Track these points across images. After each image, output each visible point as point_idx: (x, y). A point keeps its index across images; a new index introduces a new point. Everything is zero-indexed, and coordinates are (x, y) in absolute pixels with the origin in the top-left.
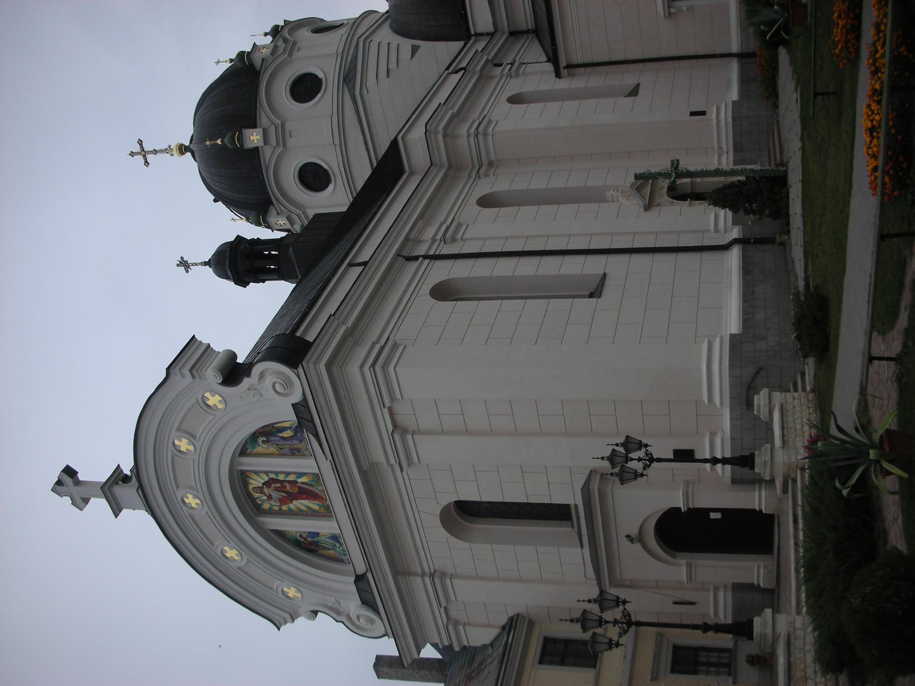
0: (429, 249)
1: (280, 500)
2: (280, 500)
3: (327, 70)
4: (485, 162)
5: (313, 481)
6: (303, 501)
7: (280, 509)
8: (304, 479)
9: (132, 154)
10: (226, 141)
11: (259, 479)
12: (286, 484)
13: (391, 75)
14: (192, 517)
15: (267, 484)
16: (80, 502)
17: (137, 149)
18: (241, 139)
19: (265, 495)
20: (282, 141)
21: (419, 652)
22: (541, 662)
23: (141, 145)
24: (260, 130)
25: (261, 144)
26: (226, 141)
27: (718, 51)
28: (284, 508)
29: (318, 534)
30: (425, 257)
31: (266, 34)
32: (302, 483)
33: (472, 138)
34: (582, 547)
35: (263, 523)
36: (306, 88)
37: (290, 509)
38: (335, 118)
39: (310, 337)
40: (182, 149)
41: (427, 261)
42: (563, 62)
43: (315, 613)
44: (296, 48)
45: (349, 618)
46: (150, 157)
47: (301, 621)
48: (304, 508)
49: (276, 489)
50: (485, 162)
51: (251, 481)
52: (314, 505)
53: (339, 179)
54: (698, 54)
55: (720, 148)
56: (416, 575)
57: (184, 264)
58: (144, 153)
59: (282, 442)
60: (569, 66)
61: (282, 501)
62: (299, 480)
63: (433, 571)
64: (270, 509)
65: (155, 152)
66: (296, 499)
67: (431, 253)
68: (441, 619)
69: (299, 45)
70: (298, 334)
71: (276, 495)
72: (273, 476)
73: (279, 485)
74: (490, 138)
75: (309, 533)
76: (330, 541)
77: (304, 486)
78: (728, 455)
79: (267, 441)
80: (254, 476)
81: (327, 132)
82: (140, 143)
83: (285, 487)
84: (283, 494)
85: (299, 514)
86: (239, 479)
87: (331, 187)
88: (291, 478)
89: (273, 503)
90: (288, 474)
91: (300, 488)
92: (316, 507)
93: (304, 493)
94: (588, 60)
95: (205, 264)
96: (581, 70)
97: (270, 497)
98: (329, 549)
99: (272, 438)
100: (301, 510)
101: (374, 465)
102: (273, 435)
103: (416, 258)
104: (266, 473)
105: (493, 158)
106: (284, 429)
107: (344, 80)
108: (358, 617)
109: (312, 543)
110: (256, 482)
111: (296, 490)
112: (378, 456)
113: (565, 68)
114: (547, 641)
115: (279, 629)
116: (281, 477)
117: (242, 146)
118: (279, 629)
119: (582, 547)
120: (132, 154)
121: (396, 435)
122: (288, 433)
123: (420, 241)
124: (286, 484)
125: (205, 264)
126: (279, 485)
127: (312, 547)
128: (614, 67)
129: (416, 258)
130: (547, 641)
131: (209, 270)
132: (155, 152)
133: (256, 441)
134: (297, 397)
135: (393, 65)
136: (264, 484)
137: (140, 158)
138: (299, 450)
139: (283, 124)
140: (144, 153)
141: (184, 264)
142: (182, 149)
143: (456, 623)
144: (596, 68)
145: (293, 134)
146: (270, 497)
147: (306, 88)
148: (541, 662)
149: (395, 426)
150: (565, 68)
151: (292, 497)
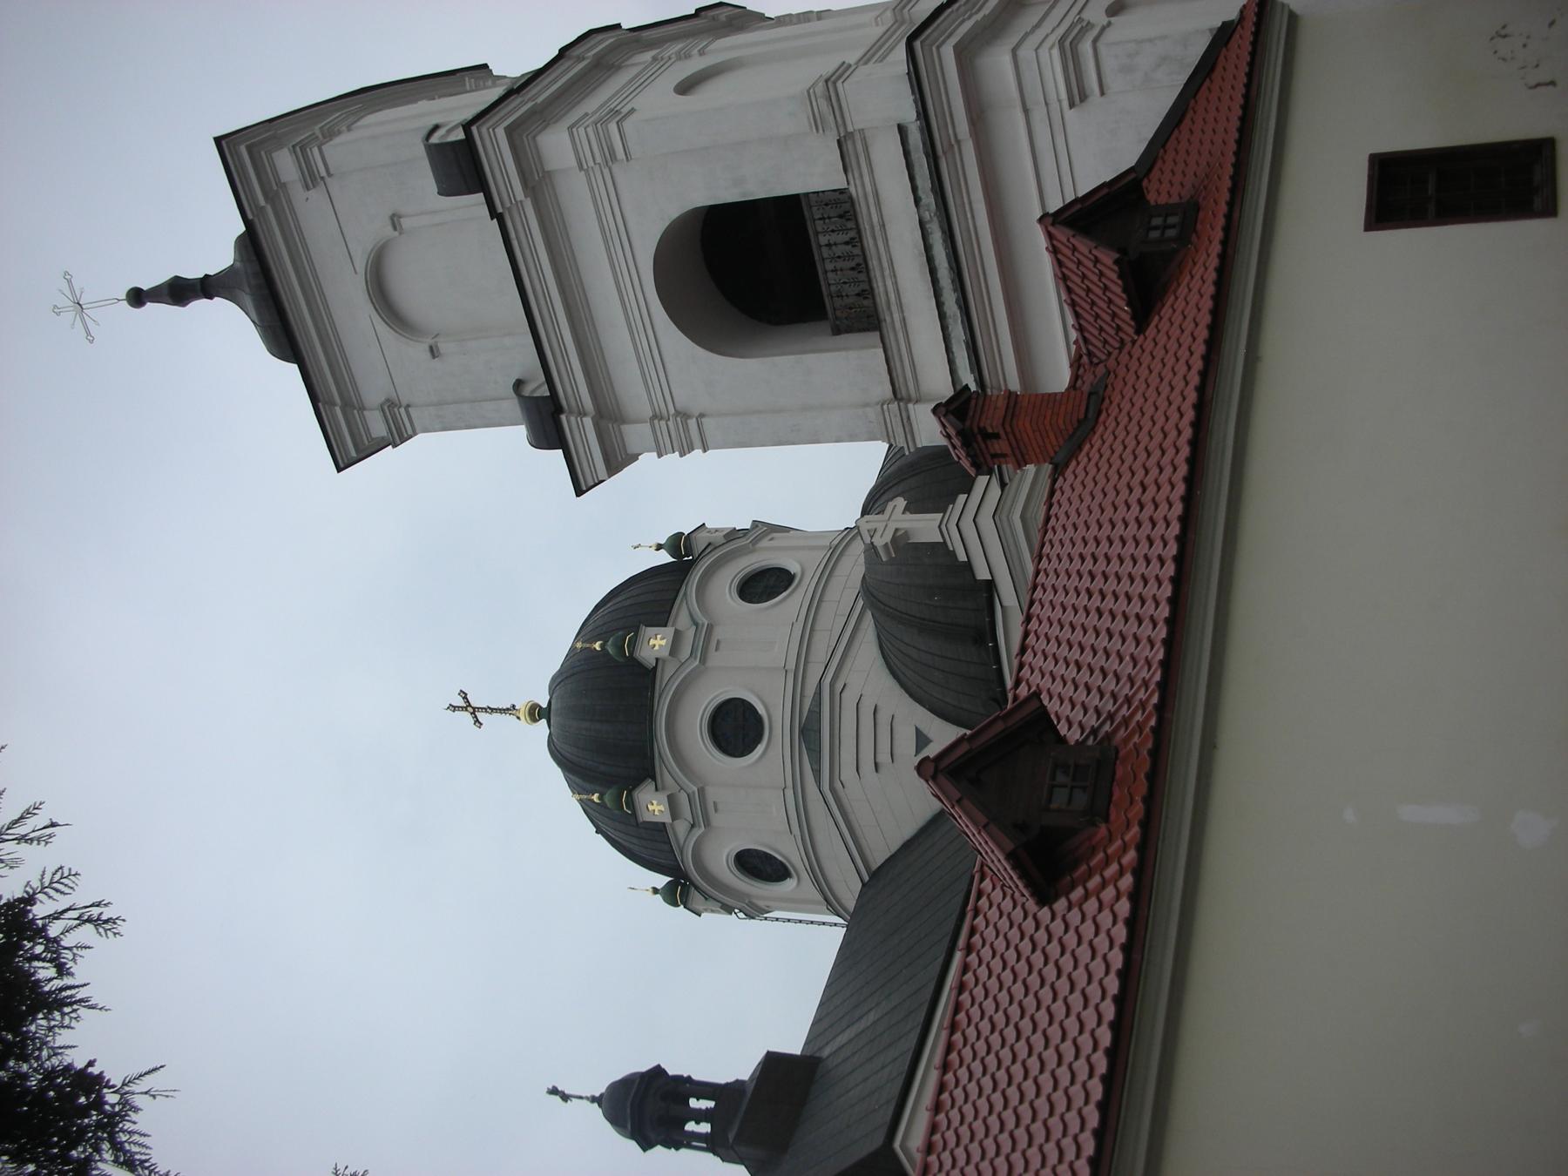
9: (454, 708)
10: (607, 798)
13: (882, 770)
17: (460, 702)
18: (631, 803)
20: (703, 815)
23: (465, 698)
24: (663, 797)
25: (667, 819)
26: (607, 798)
31: (659, 547)
36: (736, 727)
38: (789, 793)
40: (536, 713)
44: (713, 644)
53: (804, 875)
69: (718, 633)
81: (778, 813)
95: (593, 1099)
107: (802, 731)
117: (634, 814)
120: (454, 708)
125: (593, 1099)
131: (596, 1111)
135: (884, 757)
137: (466, 717)
139: (701, 791)
142: (536, 713)
145: (720, 807)
147: (736, 727)
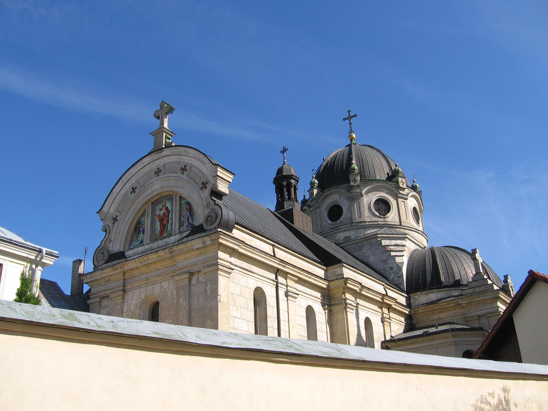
0: (282, 284)
1: (160, 215)
2: (160, 215)
3: (392, 217)
8: (169, 227)
9: (349, 111)
16: (157, 115)
28: (156, 217)
29: (143, 233)
30: (277, 283)
39: (234, 231)
41: (275, 284)
43: (106, 231)
46: (347, 121)
47: (101, 224)
49: (164, 213)
57: (284, 151)
58: (349, 118)
59: (186, 217)
65: (350, 124)
67: (279, 285)
70: (236, 225)
71: (162, 212)
79: (187, 210)
82: (355, 116)
85: (153, 223)
87: (329, 222)
88: (170, 222)
90: (172, 220)
93: (163, 227)
102: (190, 213)
103: (276, 278)
104: (172, 209)
106: (192, 219)
109: (139, 230)
111: (165, 223)
120: (349, 111)
122: (190, 219)
123: (286, 279)
127: (137, 230)
129: (276, 278)
132: (350, 124)
134: (205, 227)
137: (347, 116)
140: (349, 118)
141: (284, 151)
143: (100, 302)
146: (161, 210)
151: (161, 221)
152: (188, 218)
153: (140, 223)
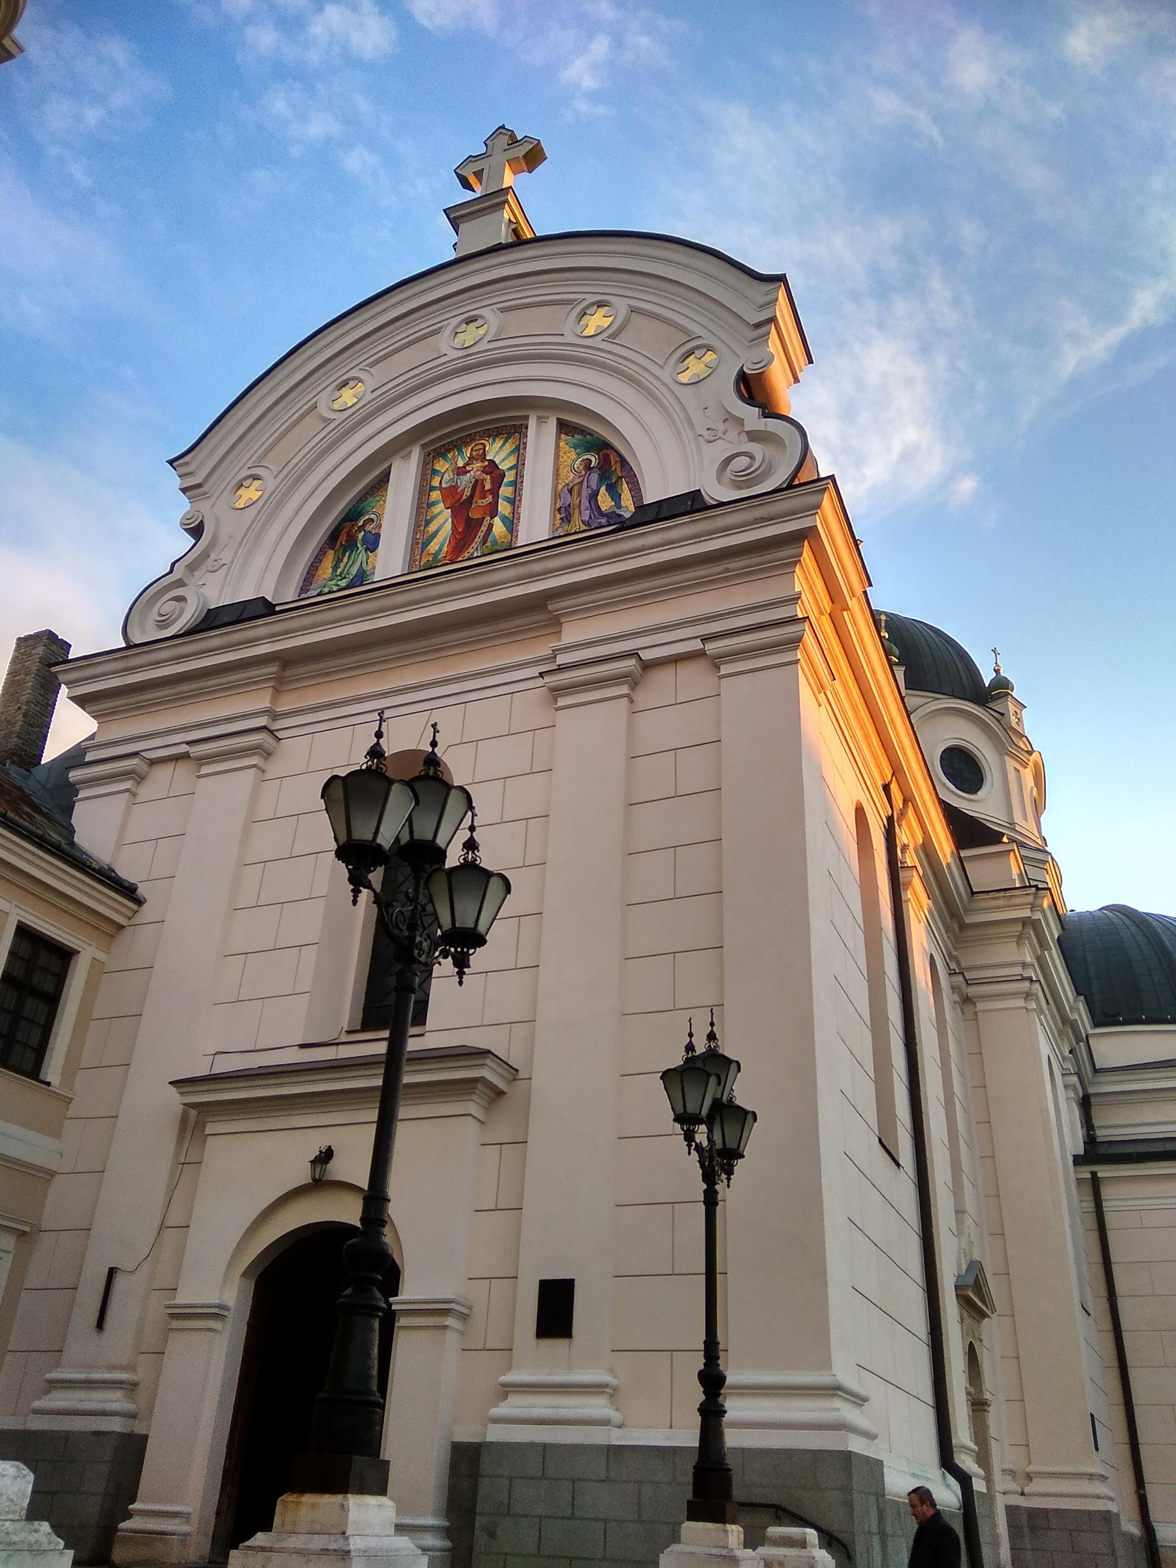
1: (454, 488)
2: (454, 488)
4: (972, 991)
5: (495, 543)
6: (448, 526)
7: (432, 489)
8: (498, 527)
11: (502, 455)
12: (490, 499)
14: (437, 331)
15: (492, 468)
19: (468, 464)
21: (82, 701)
22: (23, 931)
27: (1153, 1494)
28: (435, 495)
32: (491, 526)
33: (1018, 970)
34: (302, 1046)
35: (408, 456)
37: (431, 505)
42: (1104, 1171)
45: (180, 583)
48: (432, 528)
49: (477, 484)
50: (972, 991)
51: (499, 443)
52: (441, 542)
54: (1142, 1448)
55: (1029, 1477)
56: (274, 700)
59: (585, 493)
60: (1095, 1183)
61: (450, 493)
62: (497, 521)
63: (279, 735)
64: (434, 472)
66: (454, 516)
68: (155, 748)
71: (465, 481)
72: (510, 477)
73: (488, 486)
74: (1020, 1003)
75: (378, 536)
76: (354, 570)
77: (484, 528)
78: (733, 1439)
80: (509, 446)
83: (484, 497)
84: (467, 493)
86: (505, 419)
88: (504, 508)
89: (446, 477)
90: (514, 502)
91: (480, 522)
92: (433, 547)
93: (467, 528)
94: (1110, 1220)
96: (1090, 1205)
97: (461, 471)
98: (335, 568)
99: (595, 477)
100: (428, 523)
101: (556, 623)
102: (602, 478)
105: (981, 1006)
108: (181, 599)
110: (499, 452)
111: (475, 515)
112: (573, 632)
113: (1094, 1174)
114: (66, 955)
115: (171, 462)
116: (505, 491)
118: (171, 462)
119: (302, 1046)
121: (632, 662)
122: (605, 502)
124: (490, 499)
126: (488, 486)
127: (343, 539)
128: (1099, 1270)
130: (66, 955)
133: (588, 451)
136: (492, 462)
138: (567, 519)
143: (139, 778)
144: (1094, 1236)
146: (461, 471)
148: (23, 931)
149: (648, 666)
150: (1094, 1174)
151: (460, 507)
152: (594, 495)
153: (360, 515)
